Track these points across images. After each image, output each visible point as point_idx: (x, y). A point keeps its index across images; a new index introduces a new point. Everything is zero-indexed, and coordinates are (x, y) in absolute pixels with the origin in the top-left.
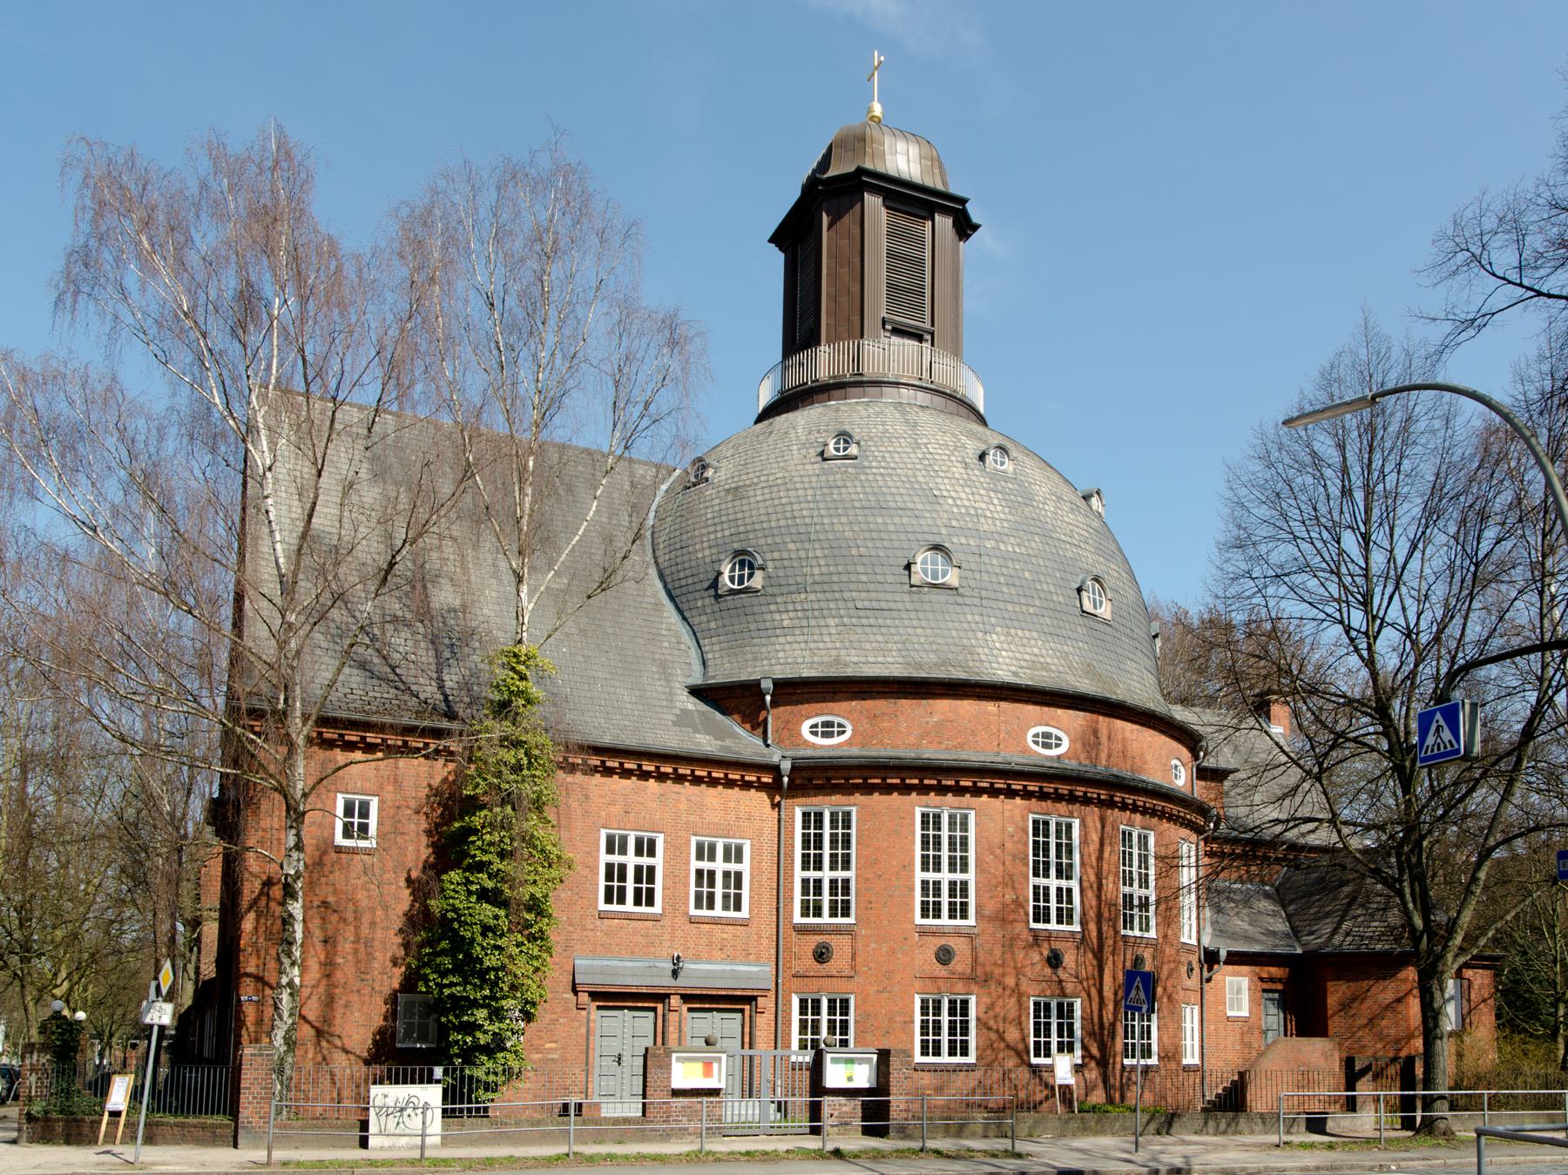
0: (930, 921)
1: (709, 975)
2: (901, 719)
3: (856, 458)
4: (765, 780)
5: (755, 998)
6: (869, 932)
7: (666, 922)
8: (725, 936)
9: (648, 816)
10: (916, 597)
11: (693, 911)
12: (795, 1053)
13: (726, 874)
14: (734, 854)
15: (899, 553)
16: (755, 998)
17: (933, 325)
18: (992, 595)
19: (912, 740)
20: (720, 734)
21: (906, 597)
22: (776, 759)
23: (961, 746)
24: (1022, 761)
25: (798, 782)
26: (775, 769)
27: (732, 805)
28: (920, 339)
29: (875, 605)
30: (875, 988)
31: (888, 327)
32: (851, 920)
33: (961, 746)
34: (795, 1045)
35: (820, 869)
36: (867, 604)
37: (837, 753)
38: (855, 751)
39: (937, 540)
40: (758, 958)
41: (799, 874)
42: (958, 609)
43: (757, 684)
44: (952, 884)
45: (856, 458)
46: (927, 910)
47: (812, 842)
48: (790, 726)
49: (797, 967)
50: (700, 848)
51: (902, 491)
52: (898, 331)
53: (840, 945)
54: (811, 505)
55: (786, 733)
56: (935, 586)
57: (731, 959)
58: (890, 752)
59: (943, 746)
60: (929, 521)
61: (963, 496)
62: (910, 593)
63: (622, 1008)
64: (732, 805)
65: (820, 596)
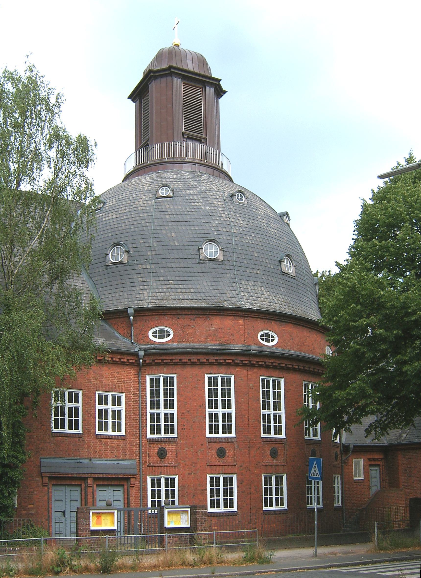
0: (214, 435)
1: (106, 467)
2: (197, 328)
3: (172, 197)
4: (131, 361)
5: (128, 479)
6: (184, 442)
7: (85, 438)
8: (114, 445)
9: (74, 382)
10: (202, 266)
11: (98, 432)
12: (149, 509)
13: (113, 412)
14: (117, 401)
15: (194, 243)
16: (128, 479)
17: (206, 136)
18: (239, 264)
19: (202, 339)
20: (109, 337)
21: (198, 265)
22: (136, 350)
23: (226, 342)
24: (256, 349)
25: (147, 362)
26: (136, 354)
27: (116, 374)
28: (200, 141)
29: (183, 270)
30: (188, 472)
31: (185, 136)
32: (175, 435)
33: (226, 342)
34: (149, 505)
35: (159, 408)
36: (179, 269)
37: (167, 346)
38: (175, 345)
39: (212, 237)
40: (130, 457)
41: (149, 411)
42: (223, 271)
43: (126, 311)
44: (224, 414)
45: (172, 197)
46: (214, 429)
47: (155, 394)
48: (143, 333)
49: (150, 461)
50: (100, 396)
51: (194, 213)
52: (190, 138)
53: (170, 449)
54: (151, 221)
55: (141, 336)
56: (212, 260)
57: (117, 458)
58: (192, 345)
59: (218, 342)
60: (208, 228)
61: (223, 215)
62: (199, 263)
63: (65, 485)
64: (116, 374)
65: (157, 266)
